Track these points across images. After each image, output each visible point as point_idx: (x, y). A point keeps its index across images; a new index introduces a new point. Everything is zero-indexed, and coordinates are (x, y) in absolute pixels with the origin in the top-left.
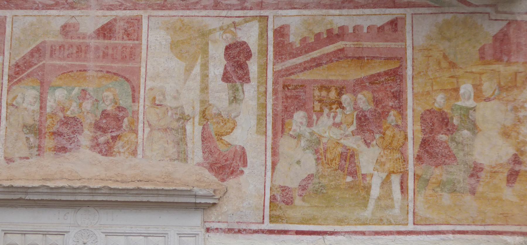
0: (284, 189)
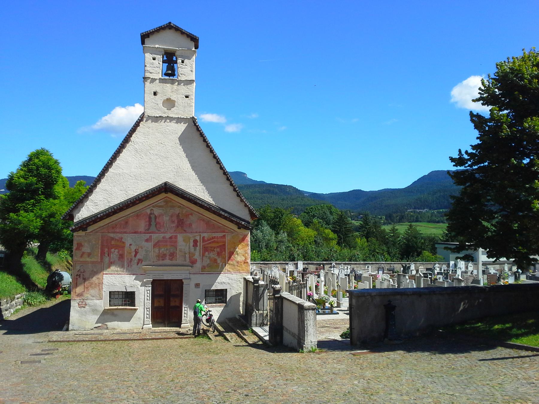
0: (204, 266)
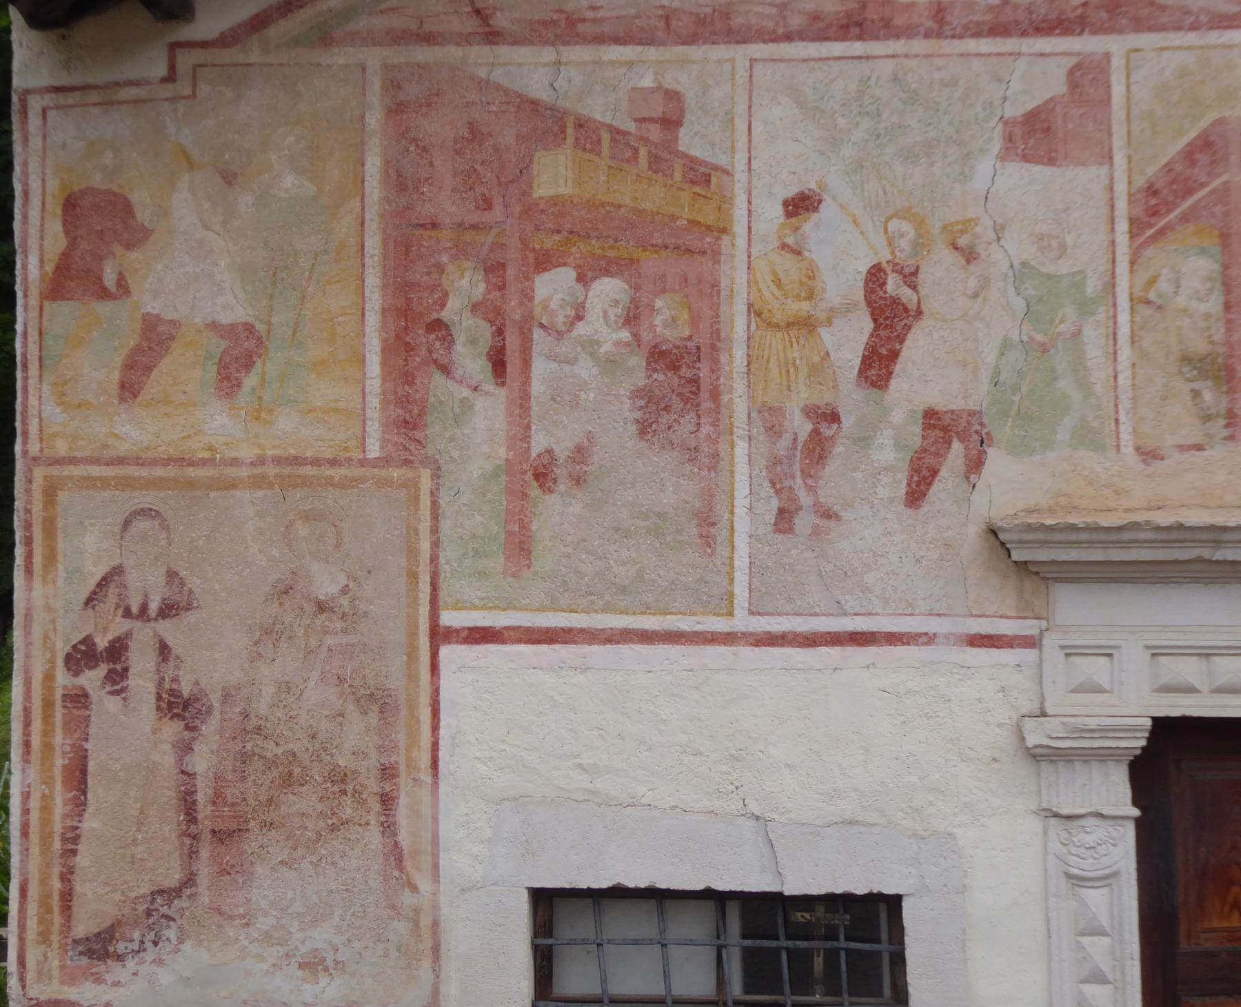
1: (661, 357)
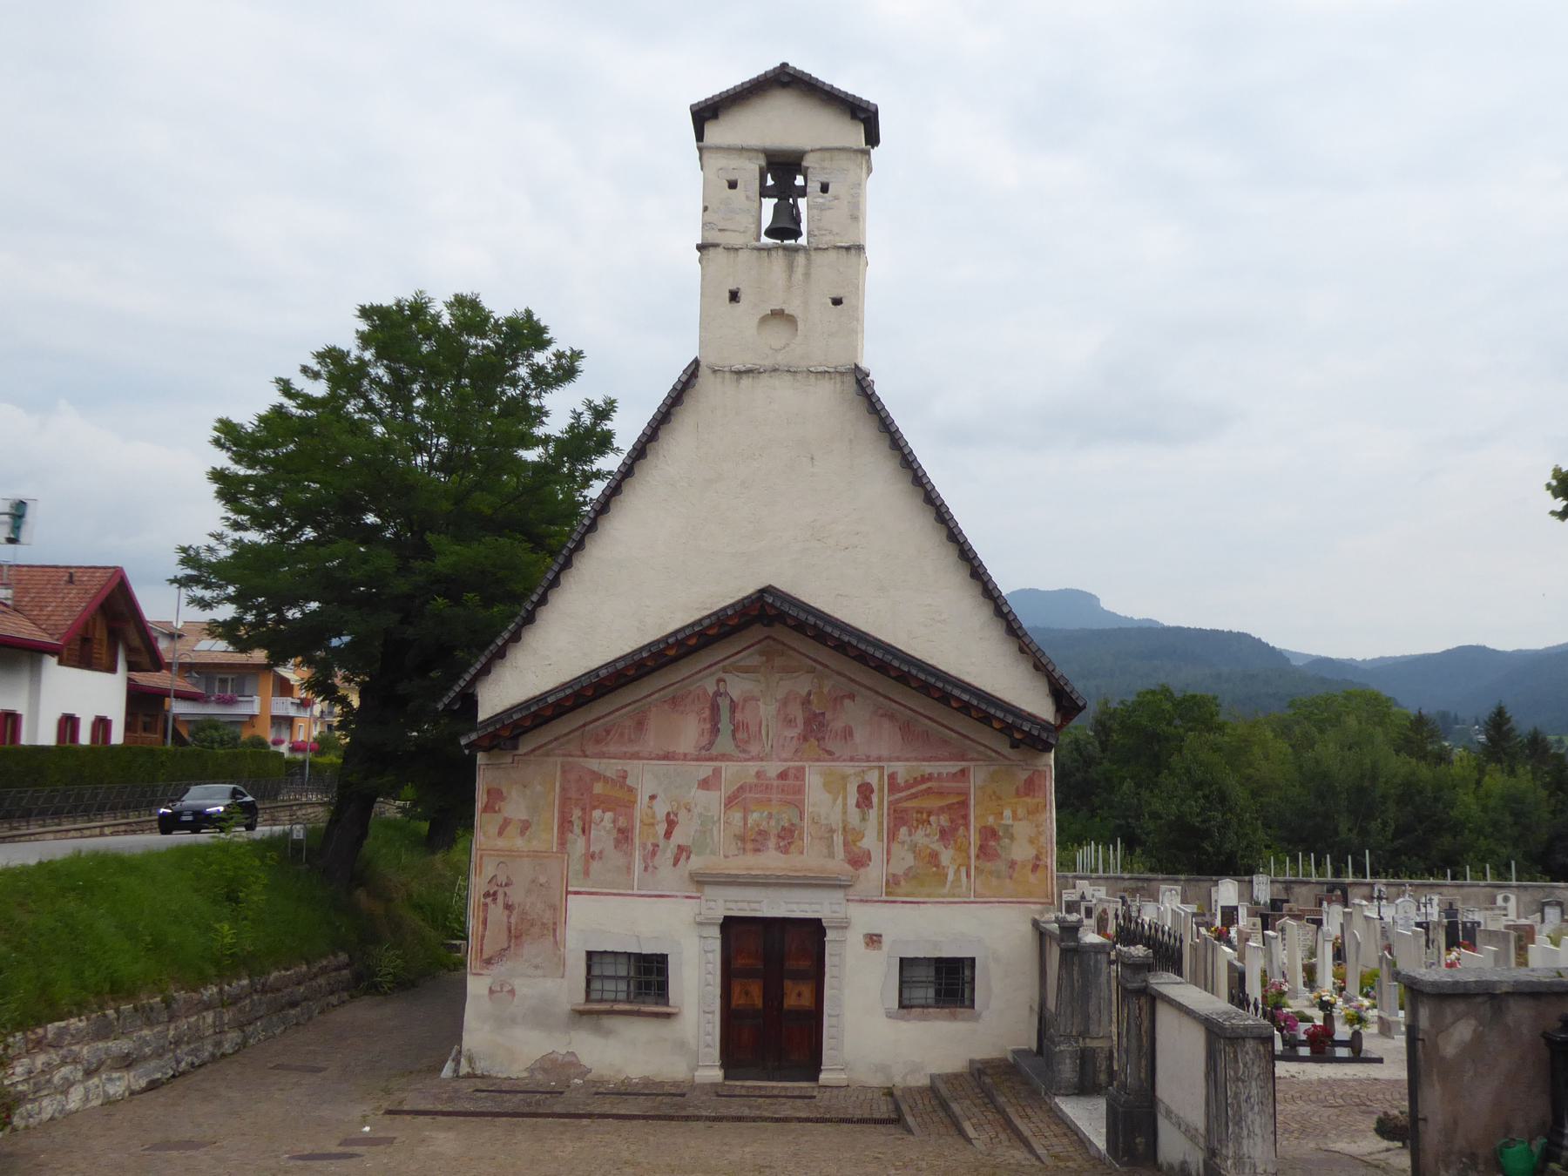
0: (894, 875)
1: (620, 831)
